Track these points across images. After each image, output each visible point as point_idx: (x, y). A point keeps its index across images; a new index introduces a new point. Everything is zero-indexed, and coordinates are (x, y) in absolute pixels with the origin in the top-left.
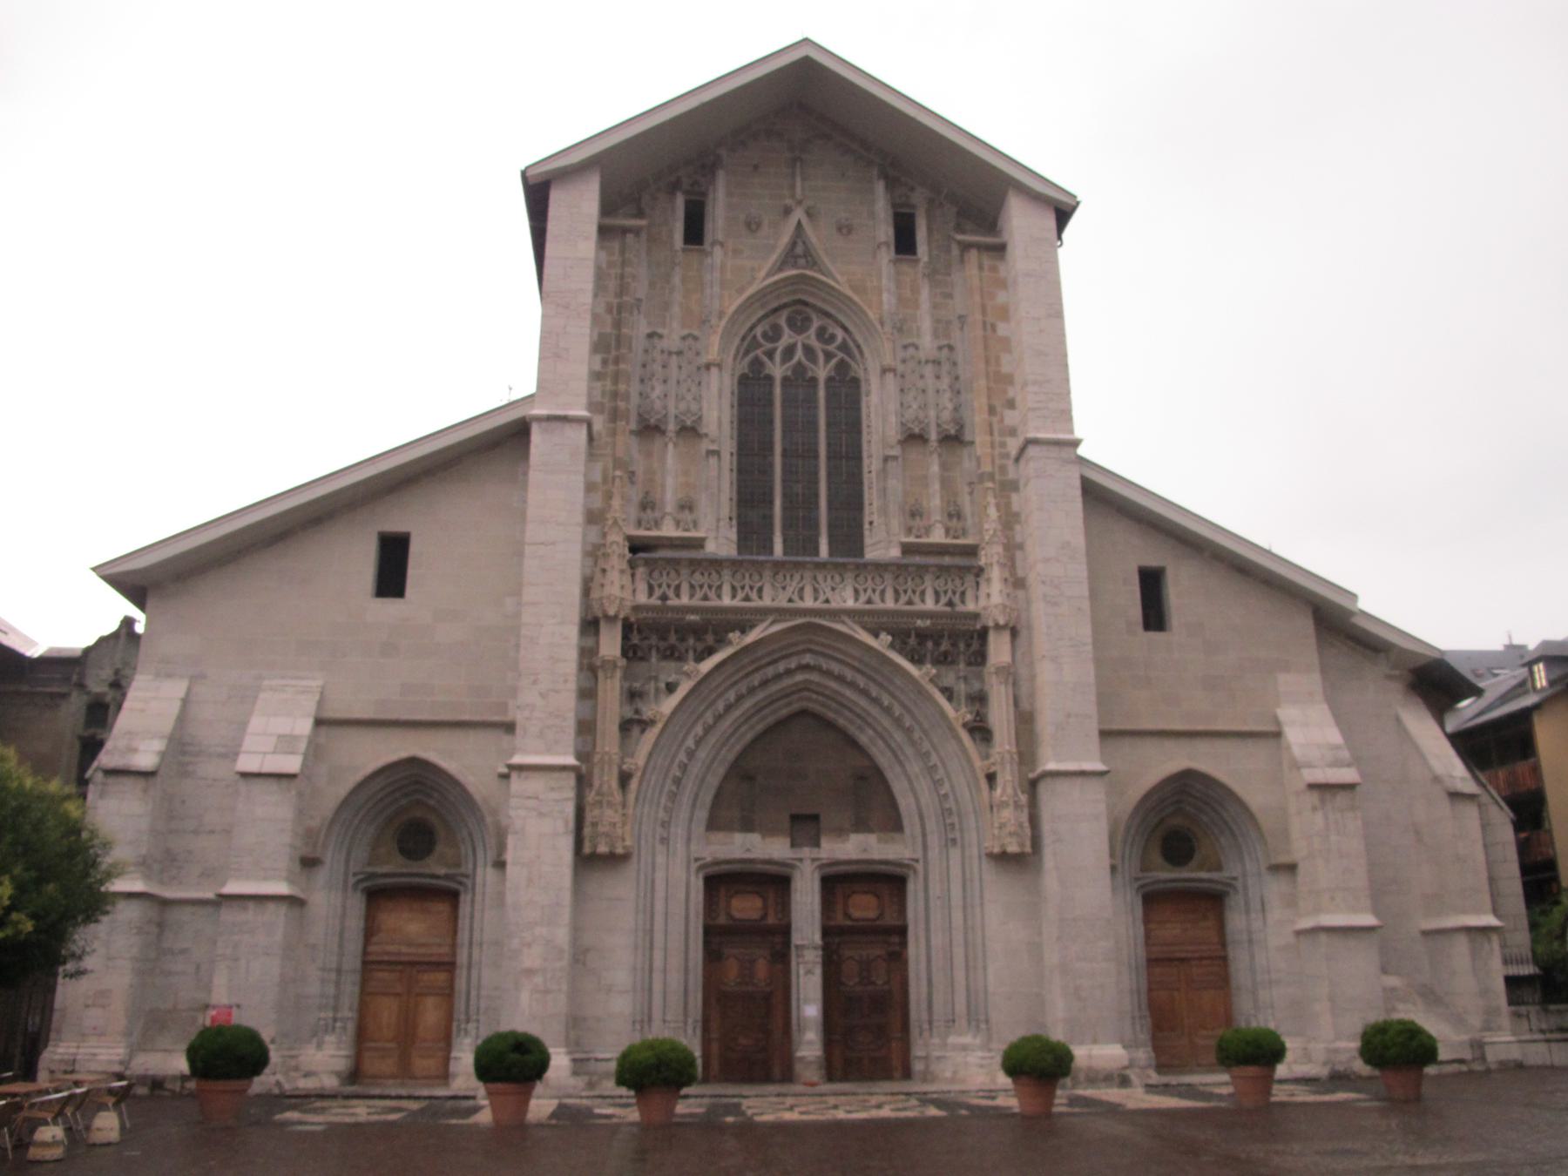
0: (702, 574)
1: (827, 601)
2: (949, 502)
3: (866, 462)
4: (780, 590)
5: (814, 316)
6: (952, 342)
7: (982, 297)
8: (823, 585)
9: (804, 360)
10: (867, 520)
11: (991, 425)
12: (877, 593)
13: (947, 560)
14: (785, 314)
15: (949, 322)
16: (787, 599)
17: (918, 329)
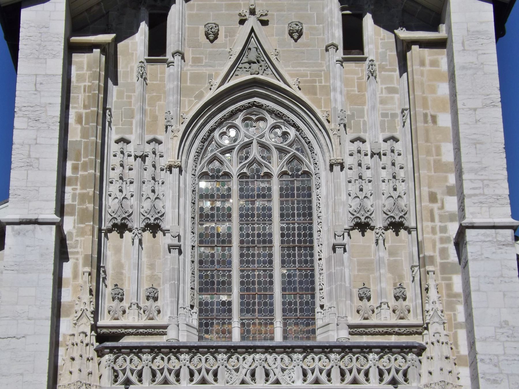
0: (162, 359)
1: (277, 382)
2: (395, 285)
3: (316, 249)
4: (233, 372)
5: (268, 116)
6: (397, 135)
7: (423, 93)
8: (273, 367)
9: (259, 158)
10: (318, 303)
11: (432, 212)
12: (324, 373)
13: (393, 339)
14: (241, 116)
15: (394, 116)
16: (240, 381)
17: (365, 123)
